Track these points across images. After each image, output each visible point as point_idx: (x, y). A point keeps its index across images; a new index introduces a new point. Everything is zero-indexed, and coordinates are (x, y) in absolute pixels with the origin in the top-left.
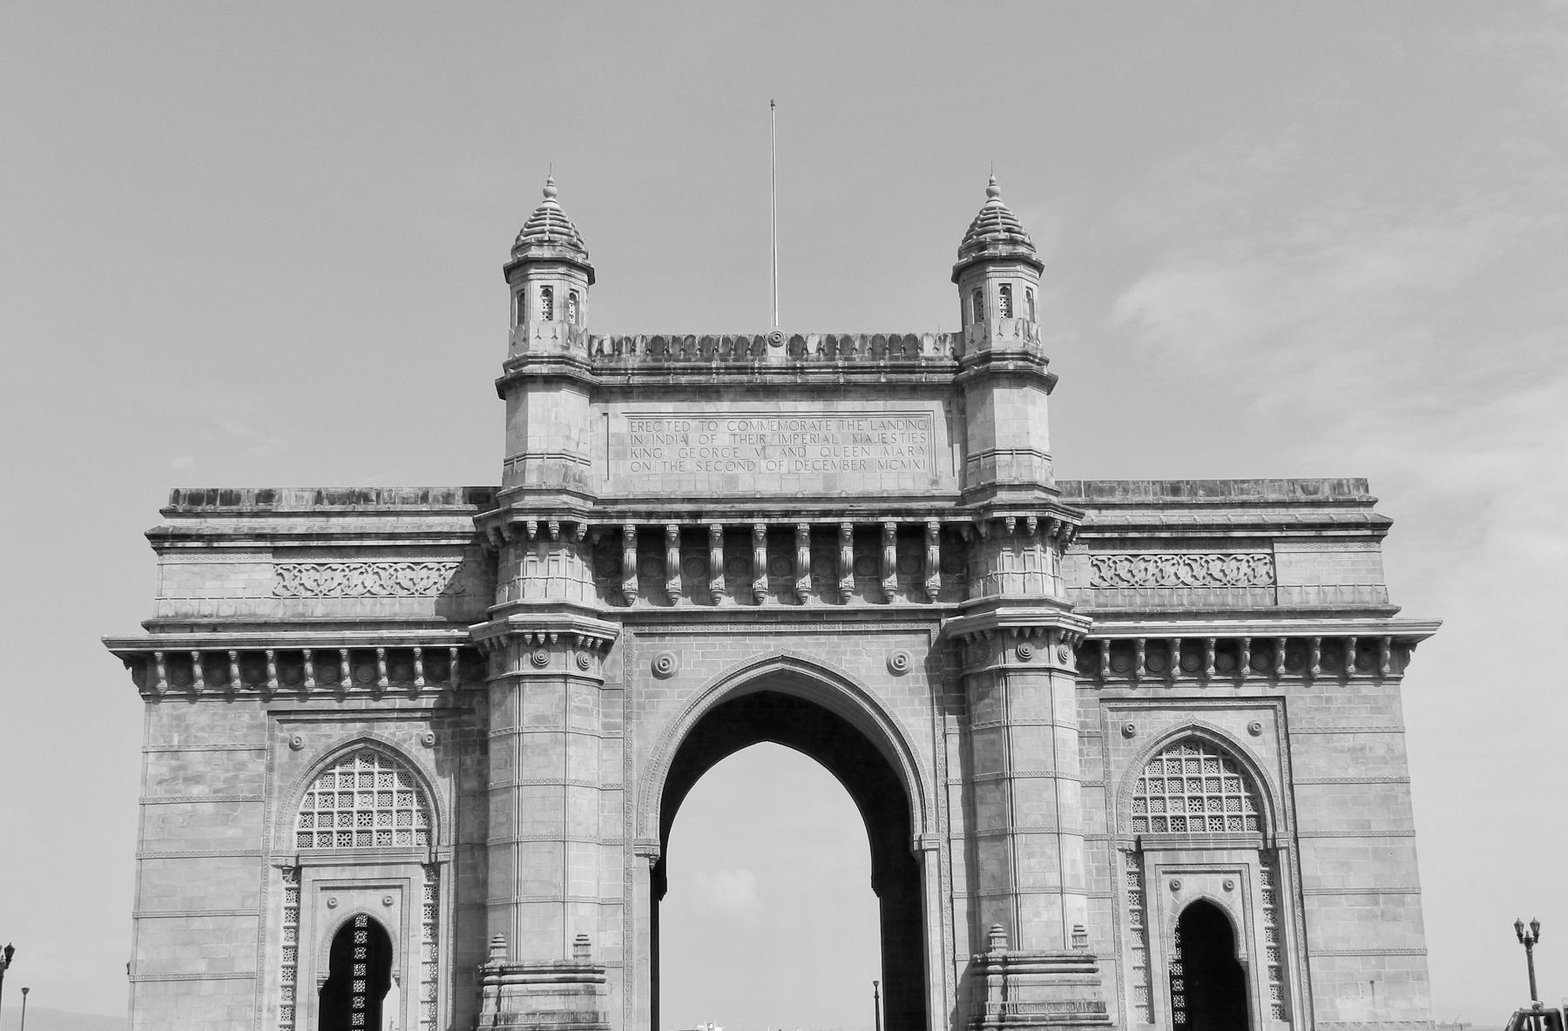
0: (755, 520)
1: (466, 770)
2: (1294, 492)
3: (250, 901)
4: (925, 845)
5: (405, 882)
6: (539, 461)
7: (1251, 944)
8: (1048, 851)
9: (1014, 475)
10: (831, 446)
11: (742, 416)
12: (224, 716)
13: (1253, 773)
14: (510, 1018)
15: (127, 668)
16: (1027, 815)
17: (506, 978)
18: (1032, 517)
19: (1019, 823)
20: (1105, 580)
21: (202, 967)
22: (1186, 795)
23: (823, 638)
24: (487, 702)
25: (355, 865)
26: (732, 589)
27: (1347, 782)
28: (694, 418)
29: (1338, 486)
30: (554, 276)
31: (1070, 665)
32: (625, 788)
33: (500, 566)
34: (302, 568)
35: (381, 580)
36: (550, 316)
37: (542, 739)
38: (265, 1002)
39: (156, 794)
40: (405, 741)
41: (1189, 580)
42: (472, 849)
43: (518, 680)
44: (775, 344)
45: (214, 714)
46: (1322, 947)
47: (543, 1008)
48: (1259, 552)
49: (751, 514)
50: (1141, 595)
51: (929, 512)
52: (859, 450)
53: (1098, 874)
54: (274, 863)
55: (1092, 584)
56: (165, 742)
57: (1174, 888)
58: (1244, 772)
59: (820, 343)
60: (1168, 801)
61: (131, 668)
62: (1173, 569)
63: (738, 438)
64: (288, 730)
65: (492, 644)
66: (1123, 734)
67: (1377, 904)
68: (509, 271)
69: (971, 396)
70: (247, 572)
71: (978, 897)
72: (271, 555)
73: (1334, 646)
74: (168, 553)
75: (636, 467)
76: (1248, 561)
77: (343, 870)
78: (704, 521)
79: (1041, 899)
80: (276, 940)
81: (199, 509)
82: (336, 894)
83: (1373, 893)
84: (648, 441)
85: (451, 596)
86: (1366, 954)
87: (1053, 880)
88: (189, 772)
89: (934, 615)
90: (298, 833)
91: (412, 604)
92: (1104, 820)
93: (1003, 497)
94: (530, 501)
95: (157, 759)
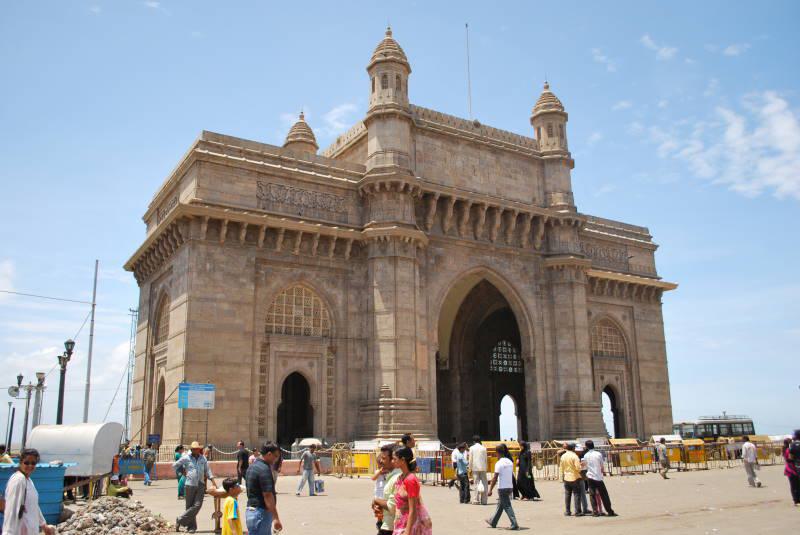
48: (623, 250)
57: (602, 378)
73: (650, 289)
77: (290, 346)
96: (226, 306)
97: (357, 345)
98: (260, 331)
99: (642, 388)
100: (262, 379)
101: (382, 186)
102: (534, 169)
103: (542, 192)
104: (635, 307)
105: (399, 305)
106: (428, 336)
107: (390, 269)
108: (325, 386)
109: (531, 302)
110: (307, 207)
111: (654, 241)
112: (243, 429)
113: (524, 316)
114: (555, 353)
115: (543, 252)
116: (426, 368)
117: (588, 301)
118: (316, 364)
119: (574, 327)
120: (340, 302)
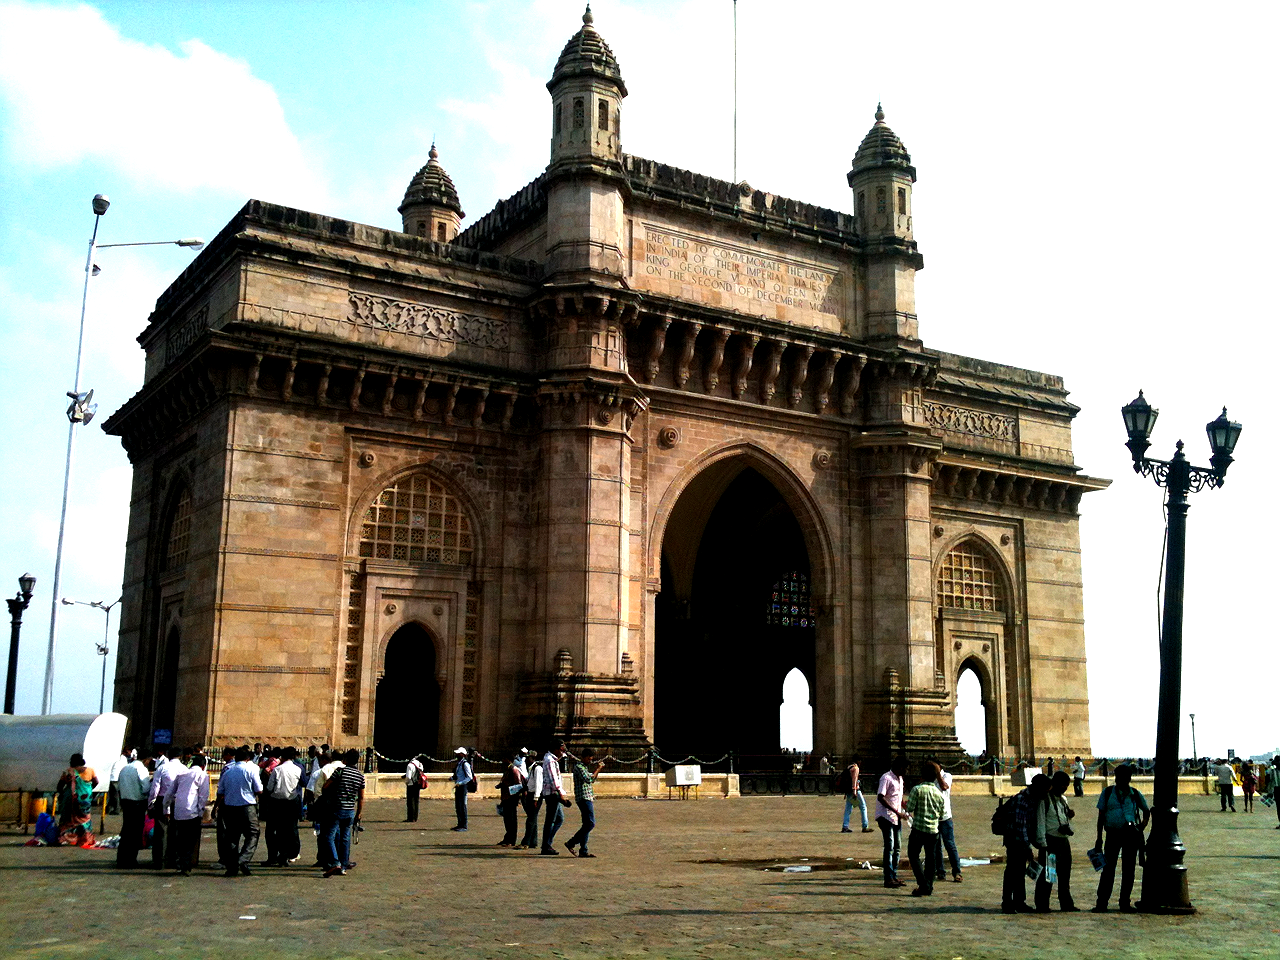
1: (510, 503)
2: (1027, 378)
3: (327, 602)
8: (926, 614)
10: (780, 284)
11: (725, 247)
12: (305, 427)
13: (1002, 570)
14: (584, 721)
21: (281, 660)
23: (774, 435)
27: (1053, 583)
28: (691, 239)
29: (1049, 379)
30: (609, 94)
32: (642, 534)
34: (374, 300)
36: (603, 125)
37: (605, 485)
38: (336, 697)
39: (241, 491)
40: (458, 471)
43: (586, 435)
44: (746, 195)
45: (297, 423)
47: (607, 713)
51: (863, 351)
52: (798, 291)
54: (347, 568)
56: (250, 442)
57: (958, 646)
58: (998, 568)
59: (773, 201)
64: (359, 447)
70: (326, 294)
71: (872, 645)
75: (650, 269)
78: (720, 326)
83: (1064, 660)
84: (659, 251)
85: (496, 350)
86: (1059, 701)
88: (273, 475)
91: (467, 352)
95: (242, 458)
96: (292, 511)
97: (519, 580)
99: (1034, 665)
100: (356, 633)
101: (569, 303)
103: (860, 313)
104: (1026, 519)
105: (593, 515)
106: (643, 565)
107: (577, 448)
108: (461, 650)
109: (831, 511)
110: (436, 338)
111: (1069, 399)
112: (317, 721)
113: (817, 534)
114: (868, 600)
116: (637, 622)
117: (933, 508)
118: (445, 608)
119: (905, 559)
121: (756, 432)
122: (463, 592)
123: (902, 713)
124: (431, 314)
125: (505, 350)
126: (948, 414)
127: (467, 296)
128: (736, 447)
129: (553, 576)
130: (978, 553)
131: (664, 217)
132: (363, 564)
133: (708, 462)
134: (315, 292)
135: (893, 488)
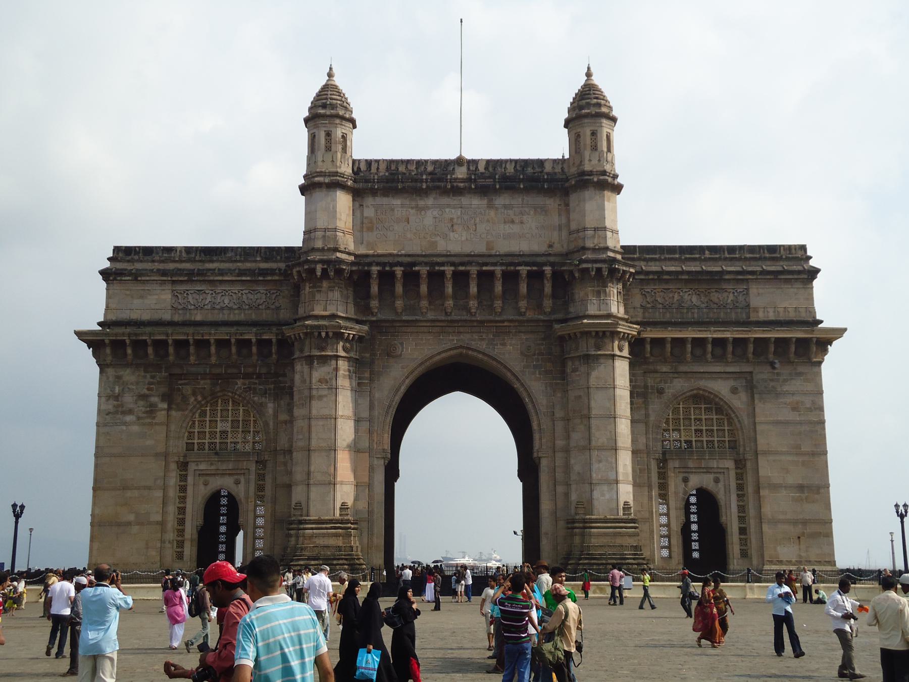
0: (445, 268)
3: (159, 481)
4: (540, 455)
5: (246, 471)
6: (323, 233)
7: (728, 514)
9: (596, 241)
12: (145, 377)
13: (733, 415)
15: (89, 349)
16: (598, 439)
17: (302, 526)
18: (604, 266)
19: (593, 443)
20: (649, 303)
21: (131, 517)
22: (693, 428)
24: (294, 371)
25: (219, 461)
26: (432, 307)
28: (412, 208)
29: (789, 248)
31: (626, 353)
33: (302, 292)
35: (233, 299)
41: (698, 303)
42: (284, 453)
45: (139, 376)
46: (770, 517)
48: (741, 287)
49: (442, 264)
50: (670, 313)
53: (640, 473)
55: (641, 305)
57: (685, 480)
60: (682, 431)
61: (91, 349)
62: (689, 297)
63: (437, 220)
65: (296, 338)
66: (657, 392)
67: (803, 493)
68: (307, 121)
69: (573, 198)
70: (157, 295)
71: (570, 485)
72: (171, 285)
74: (113, 283)
76: (733, 293)
77: (212, 464)
78: (417, 268)
79: (605, 488)
80: (175, 503)
81: (129, 258)
82: (208, 478)
83: (801, 488)
85: (273, 309)
86: (795, 523)
87: (612, 476)
88: (124, 409)
89: (549, 324)
90: (187, 443)
92: (645, 441)
93: (590, 255)
94: (317, 257)
95: (107, 400)
96: (135, 428)
97: (288, 457)
98: (175, 451)
99: (763, 493)
100: (183, 499)
102: (552, 203)
103: (564, 233)
105: (314, 412)
106: (371, 440)
107: (306, 369)
108: (251, 507)
110: (230, 309)
111: (812, 263)
112: (153, 553)
114: (567, 450)
115: (559, 316)
120: (271, 411)
121: (468, 336)
122: (253, 467)
123: (583, 535)
124: (227, 294)
125: (278, 308)
126: (671, 295)
127: (248, 278)
128: (450, 349)
129: (295, 454)
130: (710, 403)
131: (388, 196)
132: (185, 456)
133: (428, 364)
134: (150, 295)
135: (581, 365)
